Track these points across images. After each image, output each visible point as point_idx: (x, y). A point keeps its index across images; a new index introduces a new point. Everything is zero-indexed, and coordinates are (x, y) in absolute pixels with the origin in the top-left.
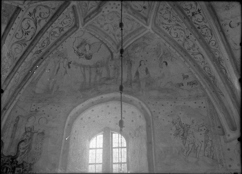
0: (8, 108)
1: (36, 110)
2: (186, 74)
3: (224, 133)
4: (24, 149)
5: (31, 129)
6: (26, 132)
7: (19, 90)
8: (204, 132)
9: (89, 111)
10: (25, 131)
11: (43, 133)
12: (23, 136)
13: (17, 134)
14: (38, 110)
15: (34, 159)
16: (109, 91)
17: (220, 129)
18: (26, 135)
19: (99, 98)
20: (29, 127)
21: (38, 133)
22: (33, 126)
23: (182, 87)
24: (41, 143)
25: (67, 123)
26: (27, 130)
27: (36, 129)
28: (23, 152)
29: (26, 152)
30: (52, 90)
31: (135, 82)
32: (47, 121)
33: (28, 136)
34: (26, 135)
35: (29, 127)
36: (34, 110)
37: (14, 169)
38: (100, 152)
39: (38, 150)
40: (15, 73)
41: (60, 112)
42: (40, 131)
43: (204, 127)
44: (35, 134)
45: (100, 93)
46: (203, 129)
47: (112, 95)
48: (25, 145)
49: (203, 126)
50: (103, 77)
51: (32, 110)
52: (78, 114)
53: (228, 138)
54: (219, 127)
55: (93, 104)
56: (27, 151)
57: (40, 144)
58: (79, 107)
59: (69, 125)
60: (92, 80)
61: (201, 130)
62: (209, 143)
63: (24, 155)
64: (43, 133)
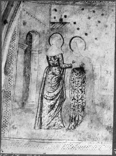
0: (12, 21)
1: (61, 20)
4: (52, 100)
6: (50, 66)
10: (48, 65)
11: (81, 70)
12: (45, 74)
15: (75, 119)
18: (51, 72)
20: (54, 57)
21: (72, 69)
22: (62, 54)
24: (81, 88)
26: (51, 62)
27: (68, 60)
28: (51, 106)
29: (57, 104)
33: (56, 75)
34: (51, 72)
35: (54, 55)
36: (57, 20)
39: (78, 101)
42: (76, 65)
44: (68, 71)
48: (54, 93)
51: (53, 20)
56: (58, 102)
57: (80, 91)
63: (55, 111)
64: (81, 70)
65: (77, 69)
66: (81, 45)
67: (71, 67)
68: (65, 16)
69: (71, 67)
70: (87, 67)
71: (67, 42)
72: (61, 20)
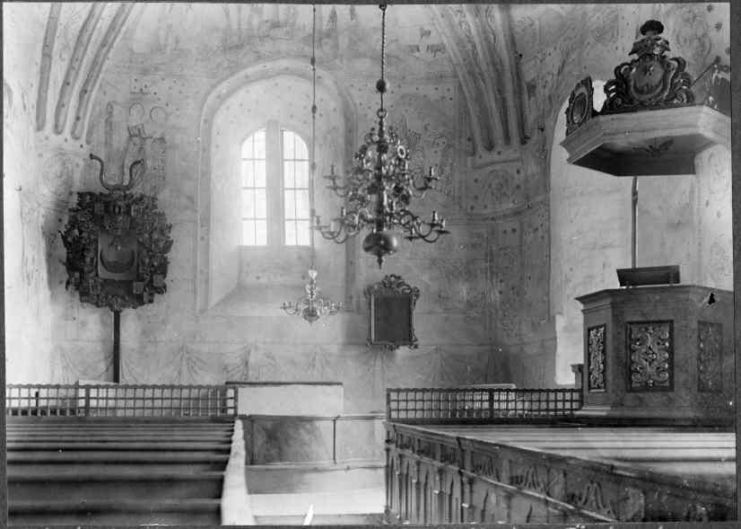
0: (91, 91)
1: (141, 90)
2: (427, 28)
3: (474, 154)
5: (139, 130)
6: (131, 136)
7: (104, 50)
8: (442, 147)
9: (242, 93)
11: (162, 139)
13: (115, 137)
14: (145, 90)
16: (278, 55)
17: (471, 143)
19: (258, 67)
23: (417, 54)
25: (203, 118)
26: (132, 133)
27: (148, 130)
30: (165, 46)
31: (328, 35)
32: (167, 116)
37: (128, 206)
38: (262, 168)
40: (97, 21)
41: (188, 97)
43: (444, 139)
44: (149, 142)
45: (259, 57)
46: (441, 144)
47: (284, 63)
49: (442, 136)
50: (265, 18)
51: (133, 90)
52: (222, 99)
53: (479, 162)
54: (469, 139)
55: (249, 80)
58: (223, 88)
59: (205, 121)
60: (244, 27)
61: (438, 144)
62: (447, 169)
64: (162, 139)
65: (158, 139)
66: (162, 115)
67: (151, 137)
68: (146, 87)
69: (151, 137)
70: (167, 138)
71: (148, 112)
72: (141, 90)
